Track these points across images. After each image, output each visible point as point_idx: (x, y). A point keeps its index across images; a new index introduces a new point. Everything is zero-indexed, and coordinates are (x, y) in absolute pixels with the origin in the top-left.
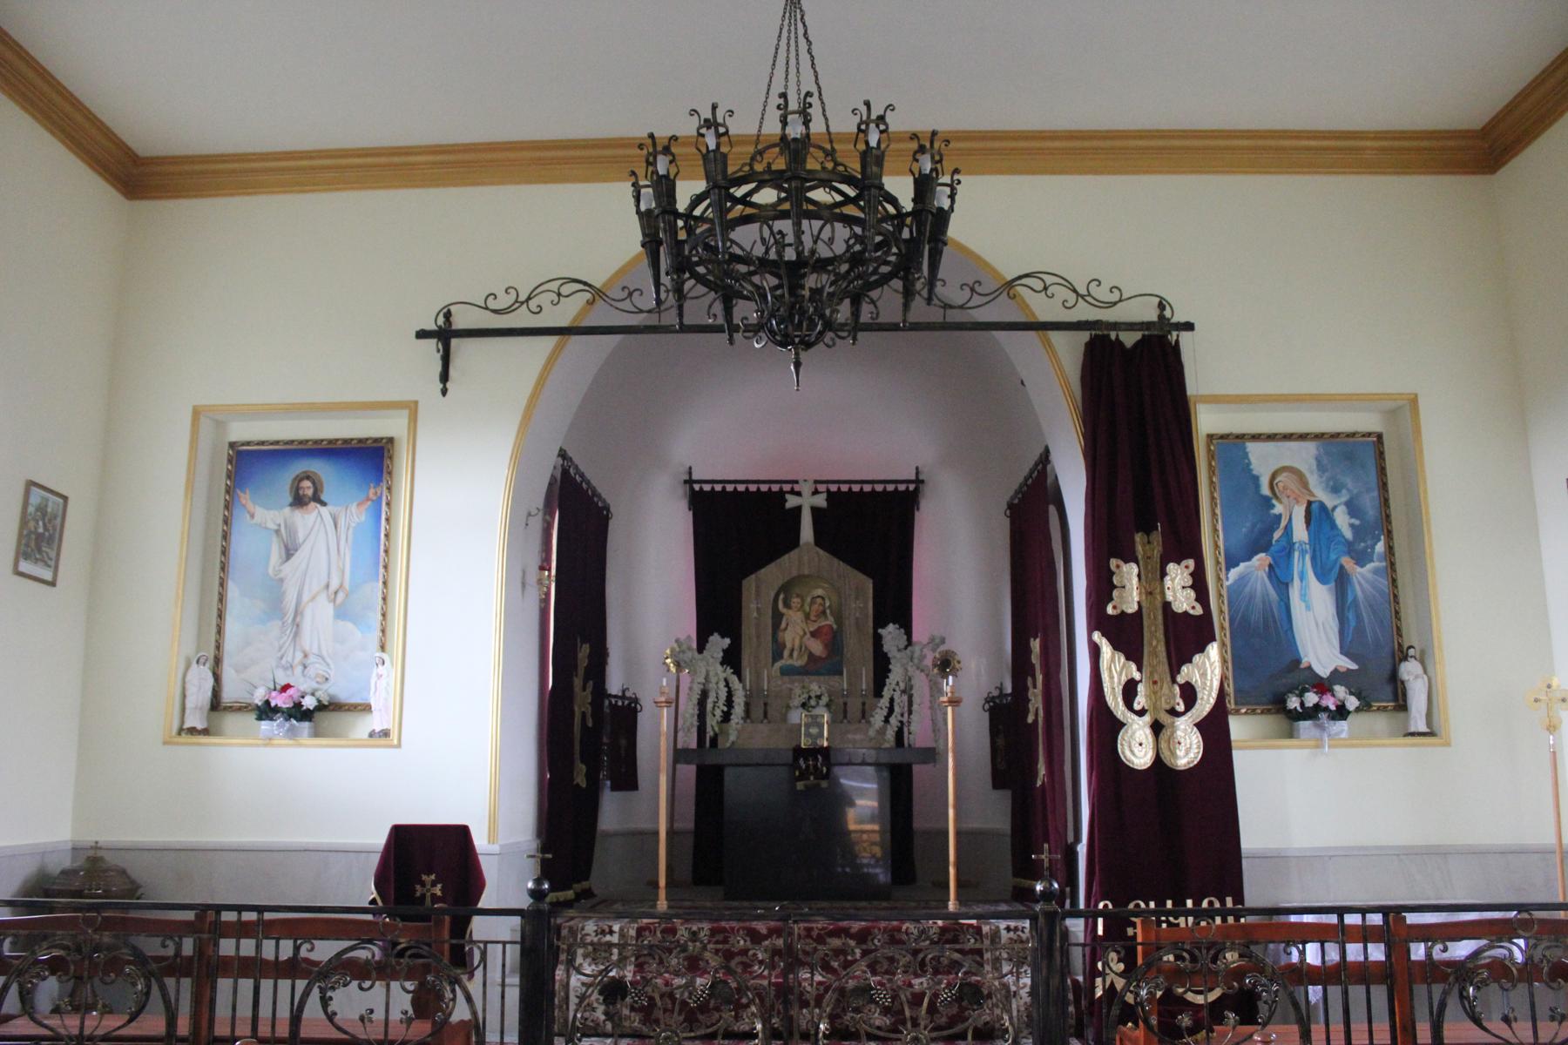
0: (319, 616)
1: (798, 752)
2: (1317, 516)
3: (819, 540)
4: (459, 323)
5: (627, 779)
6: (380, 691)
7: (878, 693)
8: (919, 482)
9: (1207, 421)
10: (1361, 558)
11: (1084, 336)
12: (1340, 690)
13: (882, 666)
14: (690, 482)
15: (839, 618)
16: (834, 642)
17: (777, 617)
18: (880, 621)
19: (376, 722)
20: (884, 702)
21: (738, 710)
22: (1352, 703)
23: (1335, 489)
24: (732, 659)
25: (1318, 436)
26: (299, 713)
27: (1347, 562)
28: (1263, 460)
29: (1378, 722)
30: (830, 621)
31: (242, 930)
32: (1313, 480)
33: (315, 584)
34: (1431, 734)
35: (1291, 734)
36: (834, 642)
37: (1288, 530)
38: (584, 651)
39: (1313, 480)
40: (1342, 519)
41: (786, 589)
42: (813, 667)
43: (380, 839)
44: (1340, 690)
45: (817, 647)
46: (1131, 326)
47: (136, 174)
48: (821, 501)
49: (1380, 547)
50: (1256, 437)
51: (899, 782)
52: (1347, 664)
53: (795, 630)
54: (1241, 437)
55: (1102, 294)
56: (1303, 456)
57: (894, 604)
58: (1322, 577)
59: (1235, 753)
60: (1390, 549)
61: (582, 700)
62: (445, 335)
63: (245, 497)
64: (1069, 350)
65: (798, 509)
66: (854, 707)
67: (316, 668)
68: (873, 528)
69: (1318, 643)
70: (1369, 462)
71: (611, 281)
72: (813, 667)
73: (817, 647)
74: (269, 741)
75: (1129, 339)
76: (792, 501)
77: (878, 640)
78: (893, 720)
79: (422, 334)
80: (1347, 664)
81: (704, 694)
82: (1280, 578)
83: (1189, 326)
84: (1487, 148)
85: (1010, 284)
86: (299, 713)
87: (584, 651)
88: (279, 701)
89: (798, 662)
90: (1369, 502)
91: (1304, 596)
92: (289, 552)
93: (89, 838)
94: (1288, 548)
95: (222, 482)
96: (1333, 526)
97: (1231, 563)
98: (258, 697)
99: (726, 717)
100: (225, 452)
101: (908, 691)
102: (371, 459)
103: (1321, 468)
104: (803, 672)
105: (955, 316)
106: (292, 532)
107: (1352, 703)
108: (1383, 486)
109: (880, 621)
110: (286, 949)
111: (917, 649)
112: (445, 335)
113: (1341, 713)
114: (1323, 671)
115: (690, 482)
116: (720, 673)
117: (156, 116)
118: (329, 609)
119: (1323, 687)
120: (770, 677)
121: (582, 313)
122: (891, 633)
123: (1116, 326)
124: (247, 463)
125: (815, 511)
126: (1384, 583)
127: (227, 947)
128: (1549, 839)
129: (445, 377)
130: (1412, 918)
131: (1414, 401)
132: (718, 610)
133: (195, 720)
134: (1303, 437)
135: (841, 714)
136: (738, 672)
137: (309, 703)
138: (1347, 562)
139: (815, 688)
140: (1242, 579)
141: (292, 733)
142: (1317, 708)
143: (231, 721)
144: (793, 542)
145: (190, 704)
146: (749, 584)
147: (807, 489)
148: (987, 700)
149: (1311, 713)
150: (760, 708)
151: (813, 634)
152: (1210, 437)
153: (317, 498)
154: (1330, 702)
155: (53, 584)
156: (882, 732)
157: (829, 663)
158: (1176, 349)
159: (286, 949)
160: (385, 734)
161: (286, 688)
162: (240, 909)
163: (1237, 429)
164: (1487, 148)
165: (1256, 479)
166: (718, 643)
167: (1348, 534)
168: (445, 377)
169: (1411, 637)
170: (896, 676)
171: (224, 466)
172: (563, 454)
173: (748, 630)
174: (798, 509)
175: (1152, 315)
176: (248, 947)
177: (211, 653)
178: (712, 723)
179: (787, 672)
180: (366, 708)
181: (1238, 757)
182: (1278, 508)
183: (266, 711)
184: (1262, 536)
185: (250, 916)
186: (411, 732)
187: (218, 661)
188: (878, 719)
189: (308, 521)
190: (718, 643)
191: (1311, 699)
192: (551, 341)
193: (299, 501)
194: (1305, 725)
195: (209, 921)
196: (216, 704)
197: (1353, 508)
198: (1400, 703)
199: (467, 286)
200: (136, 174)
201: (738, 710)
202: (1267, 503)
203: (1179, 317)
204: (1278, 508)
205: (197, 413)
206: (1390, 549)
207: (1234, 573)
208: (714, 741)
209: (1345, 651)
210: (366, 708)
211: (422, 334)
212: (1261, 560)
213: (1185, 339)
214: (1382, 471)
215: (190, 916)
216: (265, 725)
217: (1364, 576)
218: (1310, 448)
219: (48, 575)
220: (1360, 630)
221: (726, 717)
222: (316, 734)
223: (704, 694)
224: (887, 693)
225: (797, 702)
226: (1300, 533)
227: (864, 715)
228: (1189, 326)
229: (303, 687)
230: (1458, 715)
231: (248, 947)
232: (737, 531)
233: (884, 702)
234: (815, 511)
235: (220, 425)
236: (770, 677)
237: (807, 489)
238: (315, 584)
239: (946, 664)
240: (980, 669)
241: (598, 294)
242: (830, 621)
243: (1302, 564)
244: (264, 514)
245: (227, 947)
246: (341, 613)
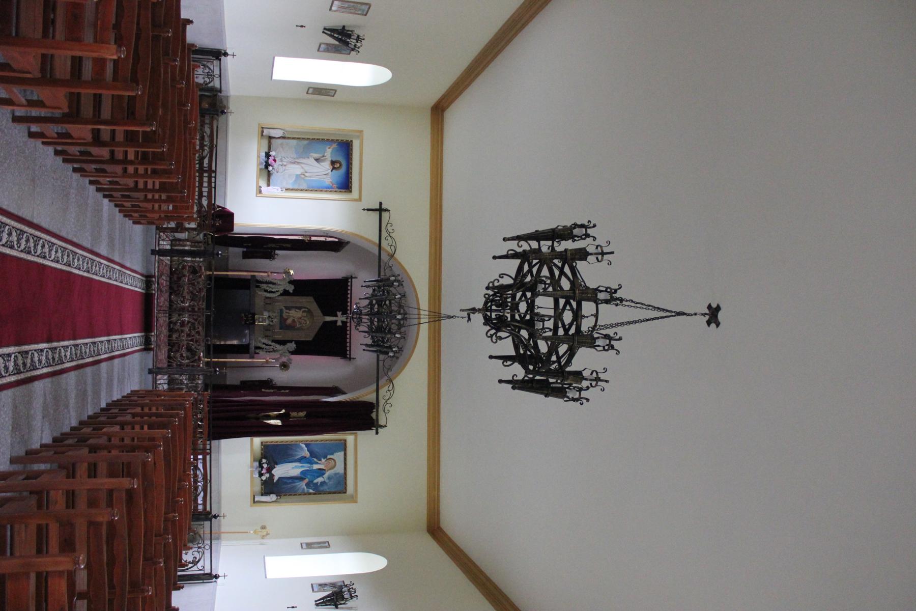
0: (296, 170)
1: (254, 315)
2: (321, 472)
3: (325, 323)
4: (384, 214)
5: (246, 256)
6: (274, 190)
7: (273, 341)
8: (350, 359)
9: (350, 438)
10: (308, 485)
11: (375, 402)
12: (268, 475)
13: (283, 343)
14: (352, 278)
15: (298, 329)
16: (291, 327)
17: (300, 308)
18: (297, 342)
19: (264, 189)
20: (270, 343)
21: (268, 295)
22: (264, 478)
23: (329, 478)
24: (286, 293)
25: (345, 473)
26: (267, 165)
27: (307, 480)
28: (338, 456)
29: (258, 487)
30: (298, 326)
31: (210, 182)
32: (332, 471)
33: (307, 168)
34: (254, 502)
35: (255, 460)
36: (291, 327)
37: (317, 463)
38: (289, 246)
39: (332, 471)
40: (320, 480)
41: (309, 311)
42: (283, 320)
43: (230, 207)
44: (268, 475)
45: (289, 321)
46: (377, 416)
47: (439, 110)
48: (339, 323)
49: (311, 491)
50: (345, 454)
51: (243, 350)
52: (276, 479)
53: (295, 314)
54: (345, 450)
55: (387, 407)
56: (339, 469)
57: (303, 348)
58: (302, 473)
59: (249, 439)
60: (310, 494)
61: (273, 246)
62: (381, 210)
63: (335, 145)
64: (371, 398)
65: (336, 316)
66: (268, 333)
67: (281, 169)
68: (331, 342)
69: (282, 471)
70: (338, 488)
71: (396, 259)
72: (283, 320)
73: (289, 321)
74: (258, 156)
75: (374, 415)
76: (339, 314)
77: (291, 341)
78: (264, 346)
79: (381, 204)
80: (276, 479)
81: (274, 284)
82: (302, 460)
83: (377, 433)
84: (435, 530)
85: (391, 381)
86: (267, 165)
87: (289, 246)
88: (271, 159)
89: (284, 315)
90: (325, 488)
91: (296, 467)
92: (317, 160)
93: (232, 106)
94: (312, 463)
95: (340, 138)
96: (318, 477)
97: (307, 445)
98: (273, 153)
99: (266, 291)
100: (350, 139)
101: (274, 351)
102: (345, 185)
103: (336, 474)
104: (281, 316)
105: (381, 363)
106: (324, 161)
107: (264, 478)
108: (330, 493)
109: (297, 342)
110: (205, 194)
111: (288, 354)
112: (381, 210)
113: (261, 475)
114: (274, 472)
115: (352, 278)
116: (281, 289)
117: (457, 119)
118: (299, 173)
119: (269, 470)
120: (280, 305)
121: (387, 251)
122: (292, 346)
123: (377, 411)
124: (346, 147)
125: (336, 322)
126: (300, 492)
127: (206, 179)
128: (223, 530)
129: (368, 210)
130: (208, 457)
131: (356, 502)
132: (302, 287)
133: (266, 132)
134: (345, 469)
135: (267, 329)
136: (281, 295)
137: (270, 168)
138: (307, 480)
139: (275, 320)
140: (302, 448)
141: (261, 164)
142: (262, 468)
143: (265, 142)
144: (325, 314)
145: (271, 131)
146: (311, 299)
147: (344, 318)
148: (271, 380)
149: (261, 466)
150: (269, 302)
151: (294, 321)
152: (345, 441)
153: (334, 168)
154: (264, 471)
155: (330, 9)
156: (260, 342)
157: (284, 325)
158: (370, 429)
159: (205, 194)
160: (260, 192)
161: (275, 161)
162: (215, 177)
163: (348, 449)
164: (435, 530)
165: (332, 454)
166: (291, 288)
167: (315, 481)
168: (368, 210)
169: (283, 499)
170: (278, 347)
171: (345, 139)
172: (348, 243)
173: (295, 298)
174: (336, 316)
175: (381, 422)
176: (205, 184)
177: (287, 136)
178: (264, 286)
179: (281, 311)
180: (269, 185)
181: (246, 440)
182: (323, 460)
183: (268, 155)
184: (315, 455)
185: (213, 185)
186: (261, 200)
187: (284, 138)
188: (264, 341)
189: (327, 165)
190: (291, 288)
191: (265, 466)
192: (377, 242)
193: (333, 163)
194: (257, 464)
195: (212, 172)
196: (270, 138)
197: (323, 483)
198: (265, 493)
199: (396, 218)
200: (439, 110)
201: (268, 295)
202: (325, 457)
203: (380, 430)
204: (323, 460)
205: (361, 132)
206: (310, 494)
207: (304, 446)
208: (258, 287)
209: (280, 479)
210: (269, 185)
211: (381, 204)
212: (307, 454)
213: (374, 432)
214: (334, 493)
215: (213, 168)
216: (264, 154)
217: (302, 485)
218: (342, 471)
219: (333, 8)
220: (286, 483)
221: (266, 291)
222: (261, 169)
223: (274, 284)
224: (273, 344)
225: (271, 314)
226: (316, 467)
227: (266, 336)
228: (377, 433)
229: (276, 166)
230: (258, 509)
231: (205, 184)
232: (332, 294)
233: (270, 343)
234: (336, 322)
235: (358, 137)
236: (280, 305)
237: (344, 318)
238: (307, 168)
239: (285, 366)
240: (281, 377)
241: (392, 256)
242: (298, 326)
243: (306, 467)
244: (329, 153)
245: (206, 179)
246: (298, 177)
